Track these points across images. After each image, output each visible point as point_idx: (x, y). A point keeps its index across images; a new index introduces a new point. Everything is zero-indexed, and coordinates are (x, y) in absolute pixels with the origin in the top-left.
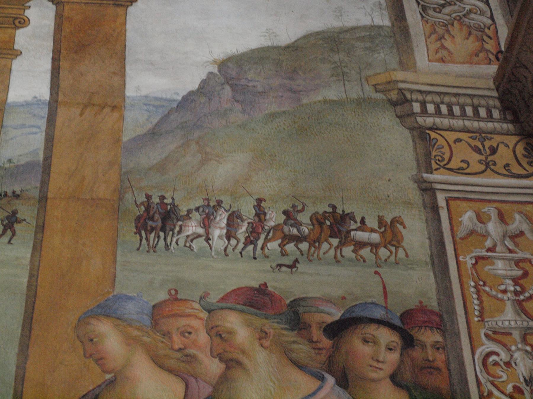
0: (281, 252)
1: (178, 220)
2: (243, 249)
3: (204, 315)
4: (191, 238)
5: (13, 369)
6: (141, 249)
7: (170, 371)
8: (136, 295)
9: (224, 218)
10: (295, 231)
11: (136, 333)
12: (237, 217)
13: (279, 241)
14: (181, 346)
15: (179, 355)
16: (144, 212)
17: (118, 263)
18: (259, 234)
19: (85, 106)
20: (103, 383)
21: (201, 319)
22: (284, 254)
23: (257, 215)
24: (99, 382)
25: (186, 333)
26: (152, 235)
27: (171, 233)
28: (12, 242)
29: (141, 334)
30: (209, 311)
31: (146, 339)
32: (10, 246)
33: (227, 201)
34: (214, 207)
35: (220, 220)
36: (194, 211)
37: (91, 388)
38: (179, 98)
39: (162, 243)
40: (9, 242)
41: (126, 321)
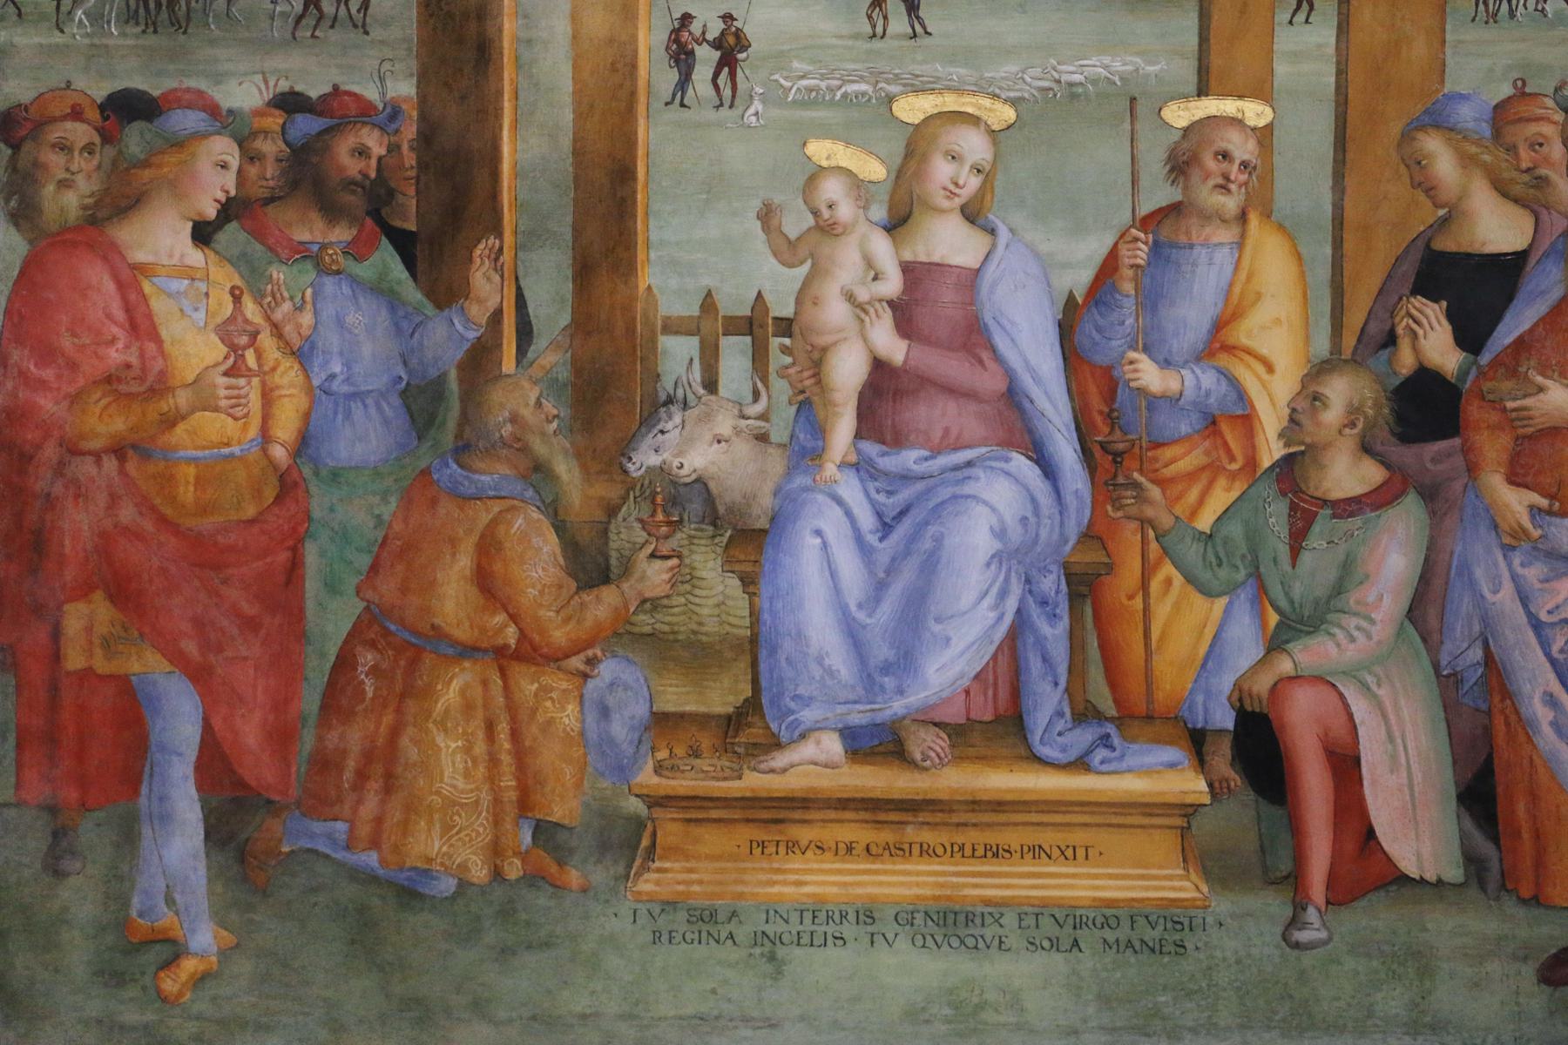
5: (1328, 208)
7: (1516, 201)
11: (1473, 149)
14: (1531, 165)
15: (1526, 178)
24: (1431, 222)
25: (1537, 144)
29: (1479, 150)
31: (1487, 158)
32: (1308, 26)
37: (1422, 229)
40: (1307, 21)
41: (1460, 133)
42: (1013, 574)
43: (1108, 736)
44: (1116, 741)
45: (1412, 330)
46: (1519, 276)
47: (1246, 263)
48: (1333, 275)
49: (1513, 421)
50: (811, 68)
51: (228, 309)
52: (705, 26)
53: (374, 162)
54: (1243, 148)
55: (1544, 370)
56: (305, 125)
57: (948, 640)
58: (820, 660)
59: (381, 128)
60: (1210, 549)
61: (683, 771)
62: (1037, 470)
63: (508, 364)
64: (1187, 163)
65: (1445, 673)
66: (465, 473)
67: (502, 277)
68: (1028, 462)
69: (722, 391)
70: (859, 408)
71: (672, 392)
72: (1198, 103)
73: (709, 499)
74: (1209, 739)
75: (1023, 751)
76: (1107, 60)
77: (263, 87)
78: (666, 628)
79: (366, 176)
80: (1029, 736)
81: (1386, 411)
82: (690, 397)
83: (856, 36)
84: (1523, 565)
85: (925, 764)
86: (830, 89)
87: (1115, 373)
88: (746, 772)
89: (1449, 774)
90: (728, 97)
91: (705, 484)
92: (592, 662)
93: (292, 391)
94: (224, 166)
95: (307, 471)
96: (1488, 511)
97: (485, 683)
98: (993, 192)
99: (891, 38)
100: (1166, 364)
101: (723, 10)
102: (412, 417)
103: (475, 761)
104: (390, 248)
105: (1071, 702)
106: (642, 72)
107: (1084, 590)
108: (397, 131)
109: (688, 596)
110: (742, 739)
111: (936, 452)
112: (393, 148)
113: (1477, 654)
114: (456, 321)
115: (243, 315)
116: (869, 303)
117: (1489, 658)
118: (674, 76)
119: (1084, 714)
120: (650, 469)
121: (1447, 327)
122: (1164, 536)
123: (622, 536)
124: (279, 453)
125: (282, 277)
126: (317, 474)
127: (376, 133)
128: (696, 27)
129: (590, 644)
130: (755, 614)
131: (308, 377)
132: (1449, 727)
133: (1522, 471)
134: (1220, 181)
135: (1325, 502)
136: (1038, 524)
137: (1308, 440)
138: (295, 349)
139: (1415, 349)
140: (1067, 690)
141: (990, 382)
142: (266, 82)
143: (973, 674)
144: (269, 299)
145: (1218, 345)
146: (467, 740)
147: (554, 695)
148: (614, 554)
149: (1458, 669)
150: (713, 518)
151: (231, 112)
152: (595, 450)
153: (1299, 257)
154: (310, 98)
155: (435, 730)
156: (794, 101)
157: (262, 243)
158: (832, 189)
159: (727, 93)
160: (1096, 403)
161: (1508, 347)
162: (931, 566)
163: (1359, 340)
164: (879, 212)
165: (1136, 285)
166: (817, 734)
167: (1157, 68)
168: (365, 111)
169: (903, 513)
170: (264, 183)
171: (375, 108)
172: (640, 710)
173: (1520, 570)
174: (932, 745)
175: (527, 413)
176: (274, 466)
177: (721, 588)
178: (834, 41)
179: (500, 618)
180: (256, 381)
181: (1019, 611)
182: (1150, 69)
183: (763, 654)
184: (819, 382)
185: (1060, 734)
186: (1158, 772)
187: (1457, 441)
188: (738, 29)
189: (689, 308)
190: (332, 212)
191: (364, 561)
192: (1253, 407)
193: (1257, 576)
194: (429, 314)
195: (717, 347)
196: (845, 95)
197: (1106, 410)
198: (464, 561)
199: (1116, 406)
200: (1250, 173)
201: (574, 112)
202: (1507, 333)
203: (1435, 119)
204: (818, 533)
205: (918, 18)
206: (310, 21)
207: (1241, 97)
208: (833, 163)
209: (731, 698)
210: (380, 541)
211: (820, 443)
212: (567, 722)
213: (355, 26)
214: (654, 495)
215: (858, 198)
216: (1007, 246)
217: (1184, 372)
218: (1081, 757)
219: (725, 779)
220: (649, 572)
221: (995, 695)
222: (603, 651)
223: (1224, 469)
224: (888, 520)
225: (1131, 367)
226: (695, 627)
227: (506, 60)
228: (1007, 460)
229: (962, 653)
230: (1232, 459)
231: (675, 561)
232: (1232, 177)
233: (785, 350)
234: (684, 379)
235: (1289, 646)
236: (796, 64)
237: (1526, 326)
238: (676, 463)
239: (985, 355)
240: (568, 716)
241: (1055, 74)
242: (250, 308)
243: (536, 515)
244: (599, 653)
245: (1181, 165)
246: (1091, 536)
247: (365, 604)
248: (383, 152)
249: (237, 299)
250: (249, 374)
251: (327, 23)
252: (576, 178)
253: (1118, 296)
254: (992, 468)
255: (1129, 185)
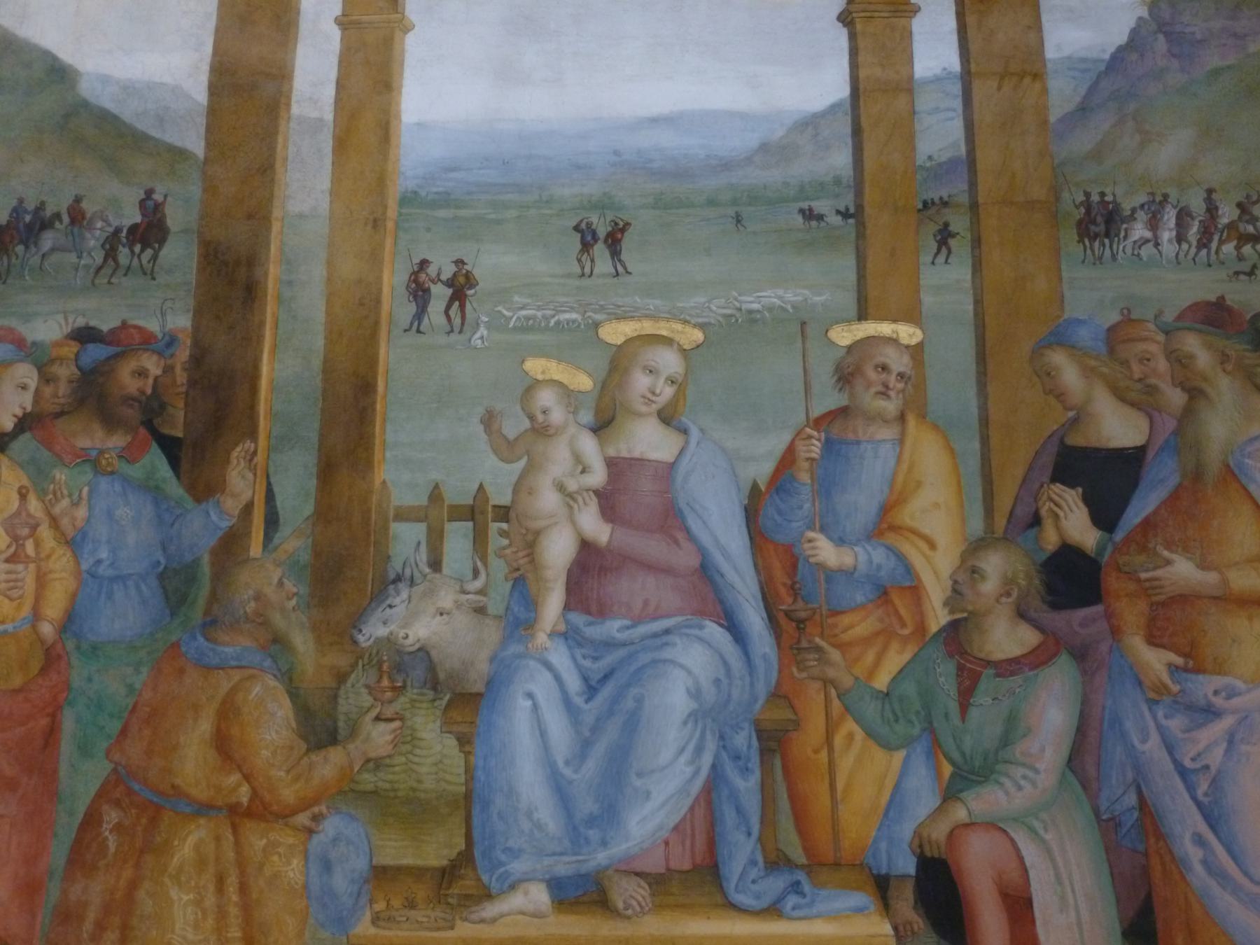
0: (1238, 256)
1: (1123, 222)
2: (1196, 254)
3: (1161, 337)
4: (1139, 243)
5: (975, 411)
6: (1086, 261)
7: (1133, 404)
8: (1087, 318)
9: (1173, 216)
10: (1250, 229)
11: (1093, 363)
12: (1186, 214)
13: (1235, 243)
14: (1142, 376)
15: (1139, 386)
16: (1085, 214)
17: (1064, 280)
18: (1212, 234)
19: (1002, 78)
20: (1066, 422)
21: (1158, 343)
22: (1240, 258)
23: (1209, 210)
25: (1145, 359)
26: (1097, 244)
27: (1116, 239)
28: (949, 261)
30: (1167, 333)
31: (1105, 370)
33: (1174, 194)
34: (1160, 203)
35: (1168, 220)
36: (1139, 210)
37: (1055, 428)
38: (1107, 56)
39: (1108, 252)
40: (946, 262)
42: (708, 732)
43: (798, 883)
44: (807, 888)
45: (1053, 511)
46: (1140, 467)
47: (906, 456)
48: (983, 465)
49: (1147, 589)
50: (529, 301)
51: (16, 504)
52: (440, 269)
53: (151, 381)
54: (899, 362)
55: (1169, 546)
56: (97, 352)
57: (648, 795)
58: (529, 814)
59: (160, 354)
60: (887, 706)
61: (399, 922)
62: (727, 635)
63: (256, 549)
64: (852, 374)
65: (1104, 817)
66: (211, 646)
67: (255, 475)
68: (720, 629)
69: (445, 570)
70: (567, 583)
71: (400, 572)
72: (858, 326)
73: (432, 668)
74: (893, 883)
75: (719, 899)
76: (780, 292)
77: (63, 322)
78: (387, 786)
79: (143, 392)
80: (725, 884)
81: (1037, 582)
82: (417, 574)
83: (569, 276)
84: (1166, 717)
85: (630, 912)
86: (545, 317)
87: (796, 551)
88: (458, 922)
89: (1113, 911)
90: (458, 323)
91: (428, 653)
92: (317, 818)
93: (64, 574)
94: (24, 387)
95: (70, 645)
96: (1131, 669)
97: (218, 839)
98: (685, 399)
99: (598, 277)
100: (840, 542)
101: (456, 256)
102: (167, 598)
103: (204, 912)
104: (159, 451)
105: (764, 850)
106: (385, 307)
107: (773, 745)
108: (172, 356)
109: (408, 755)
110: (455, 890)
111: (637, 622)
112: (168, 370)
113: (1131, 799)
114: (212, 513)
115: (26, 510)
116: (577, 492)
117: (1143, 803)
118: (412, 308)
119: (776, 862)
120: (378, 641)
121: (1085, 510)
122: (844, 695)
123: (351, 701)
124: (47, 629)
125: (63, 477)
126: (78, 648)
127: (155, 358)
128: (432, 270)
129: (316, 801)
130: (469, 770)
131: (78, 563)
132: (1111, 867)
133: (1159, 633)
134: (883, 389)
135: (988, 663)
136: (730, 685)
137: (970, 608)
138: (69, 538)
139: (1058, 528)
140: (760, 839)
141: (685, 559)
142: (66, 319)
143: (672, 825)
144: (51, 496)
145: (885, 526)
146: (199, 893)
147: (281, 850)
148: (342, 718)
149: (1117, 813)
150: (434, 683)
151: (34, 344)
152: (328, 624)
153: (952, 451)
154: (102, 331)
155: (169, 884)
156: (515, 329)
157: (50, 449)
158: (546, 398)
159: (457, 321)
160: (780, 576)
161: (1137, 526)
162: (632, 725)
163: (1009, 521)
164: (587, 417)
165: (812, 474)
166: (525, 885)
167: (823, 298)
168: (147, 340)
169: (606, 677)
170: (56, 400)
171: (156, 337)
172: (361, 864)
173: (1164, 722)
174: (634, 894)
175: (270, 591)
176: (42, 642)
177: (438, 748)
178: (548, 279)
179: (235, 778)
180: (32, 566)
181: (714, 766)
182: (817, 299)
183: (476, 811)
184: (532, 561)
185: (754, 882)
186: (848, 917)
187: (1099, 608)
188: (468, 271)
189: (419, 499)
190: (110, 422)
191: (116, 726)
192: (919, 580)
193: (931, 730)
194: (189, 507)
195: (442, 531)
196: (558, 323)
197: (789, 582)
198: (205, 726)
199: (798, 578)
200: (906, 383)
201: (326, 338)
202: (1136, 513)
203: (1059, 338)
204: (530, 695)
205: (620, 260)
206: (107, 271)
207: (895, 321)
208: (547, 377)
209: (445, 852)
210: (130, 708)
211: (532, 615)
212: (291, 875)
213: (145, 274)
214: (380, 663)
215: (568, 405)
216: (698, 443)
217: (856, 549)
218: (775, 903)
219: (438, 929)
220: (374, 734)
221: (693, 845)
222: (328, 808)
223: (897, 634)
224: (593, 683)
225: (811, 545)
226: (415, 785)
227: (269, 298)
228: (701, 627)
229: (663, 805)
230: (904, 625)
231: (397, 724)
232: (891, 386)
233: (503, 534)
234: (412, 560)
235: (964, 795)
236: (516, 298)
237: (1150, 509)
238: (402, 634)
239: (680, 536)
240: (294, 870)
241: (736, 303)
242: (34, 505)
243: (272, 683)
244: (324, 809)
245: (846, 376)
246: (778, 695)
247: (112, 766)
248: (159, 372)
249: (23, 496)
250: (27, 560)
251: (121, 272)
252: (324, 391)
253: (796, 484)
254: (688, 635)
255: (803, 394)
